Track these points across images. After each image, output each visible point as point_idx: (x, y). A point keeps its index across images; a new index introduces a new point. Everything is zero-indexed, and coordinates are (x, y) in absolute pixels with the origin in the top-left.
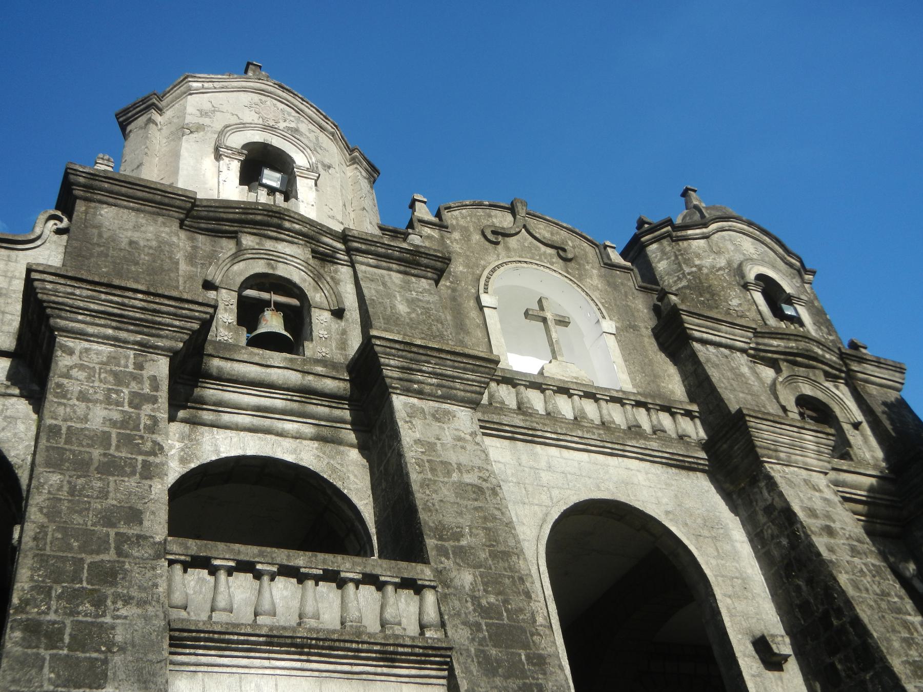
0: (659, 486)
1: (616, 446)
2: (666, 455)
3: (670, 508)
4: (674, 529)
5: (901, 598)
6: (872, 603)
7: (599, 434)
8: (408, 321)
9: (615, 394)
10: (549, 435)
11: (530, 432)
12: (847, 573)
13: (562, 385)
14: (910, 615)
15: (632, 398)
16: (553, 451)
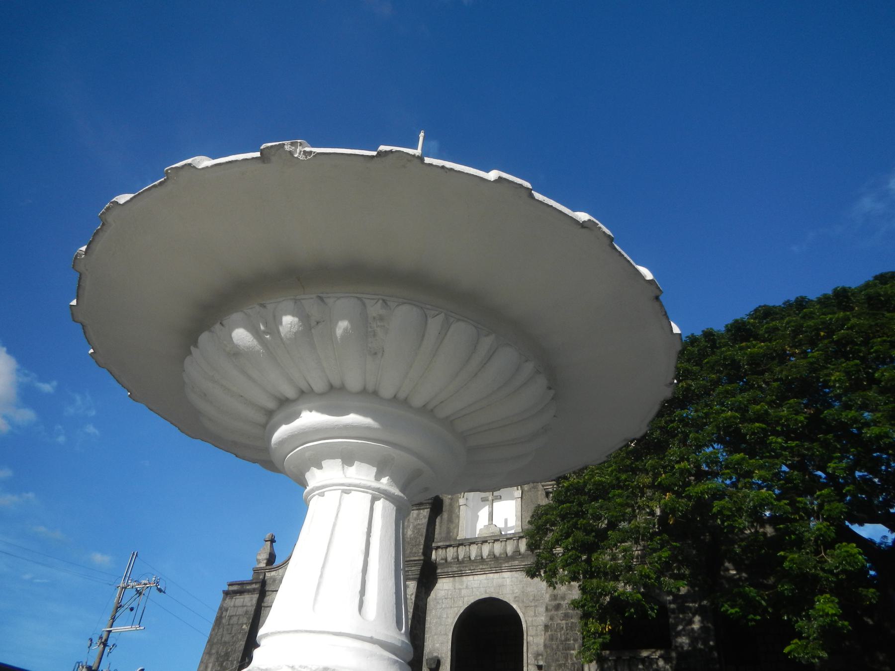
0: (516, 584)
1: (497, 569)
2: (522, 566)
3: (517, 595)
4: (515, 606)
5: (575, 640)
6: (555, 647)
7: (490, 564)
8: (409, 540)
9: (509, 536)
10: (467, 572)
11: (460, 573)
12: (551, 631)
13: (484, 540)
14: (574, 649)
15: (517, 536)
16: (471, 578)
